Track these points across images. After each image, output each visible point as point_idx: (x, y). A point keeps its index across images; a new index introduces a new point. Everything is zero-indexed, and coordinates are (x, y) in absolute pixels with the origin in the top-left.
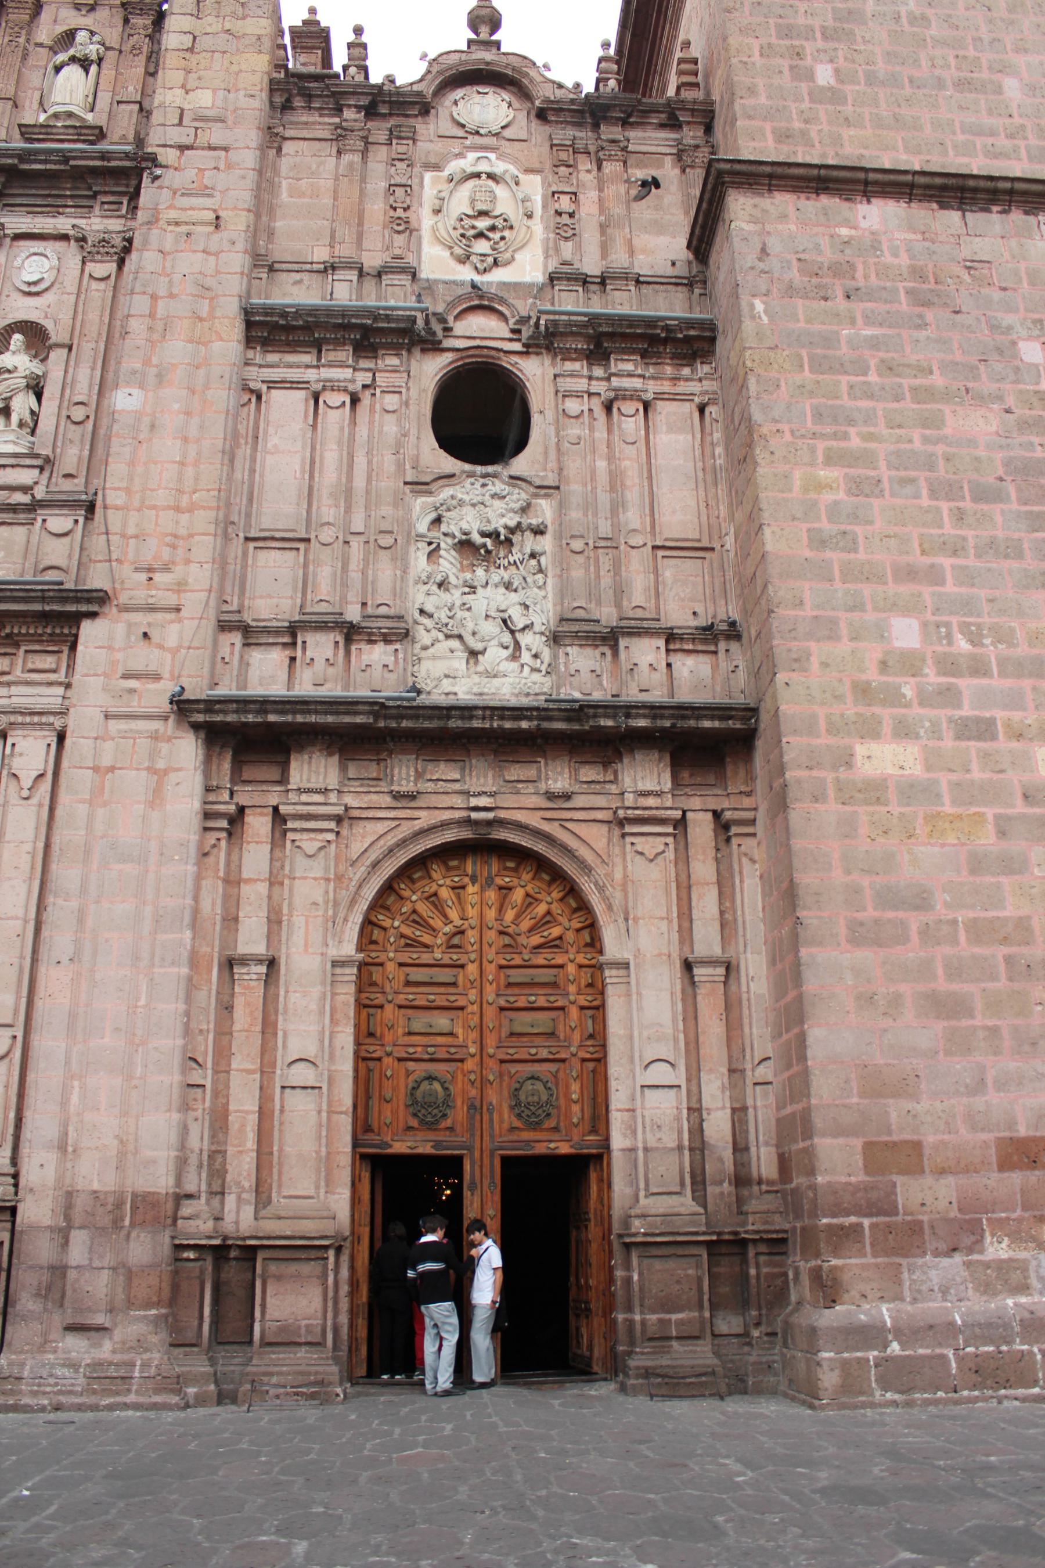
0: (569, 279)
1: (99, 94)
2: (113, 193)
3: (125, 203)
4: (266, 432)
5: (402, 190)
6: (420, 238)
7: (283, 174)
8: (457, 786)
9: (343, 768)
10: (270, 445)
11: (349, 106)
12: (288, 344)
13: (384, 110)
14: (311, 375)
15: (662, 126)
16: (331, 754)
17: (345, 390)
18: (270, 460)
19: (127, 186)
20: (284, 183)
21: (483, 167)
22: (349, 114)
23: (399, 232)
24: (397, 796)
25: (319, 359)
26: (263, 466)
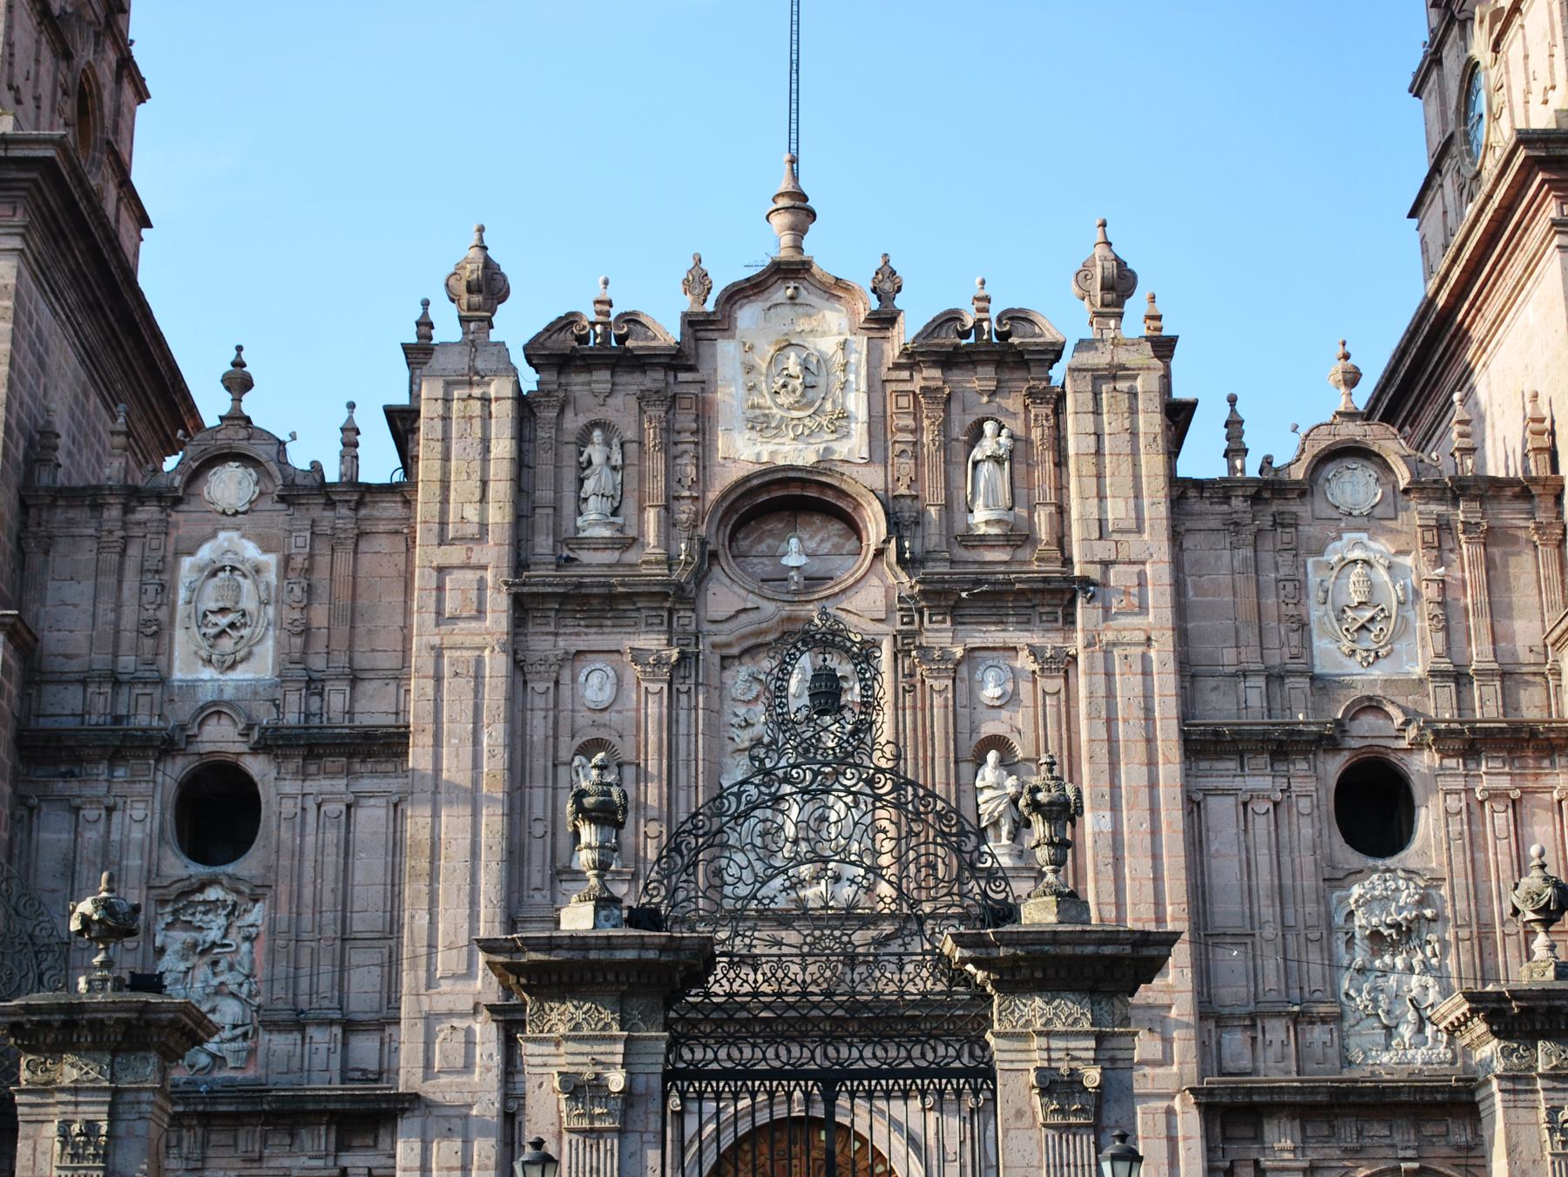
0: (1442, 676)
1: (1017, 491)
2: (1049, 605)
3: (1060, 611)
4: (1208, 838)
5: (1291, 584)
6: (1310, 631)
7: (1187, 572)
8: (1388, 1141)
9: (1303, 1129)
10: (1213, 849)
11: (1237, 496)
12: (1216, 752)
13: (1267, 495)
14: (1238, 782)
15: (1516, 497)
16: (1293, 1119)
17: (1269, 798)
18: (1213, 862)
19: (1062, 599)
20: (1189, 580)
21: (1357, 554)
22: (1238, 503)
23: (1294, 631)
24: (1345, 1150)
25: (1242, 769)
26: (1209, 869)
